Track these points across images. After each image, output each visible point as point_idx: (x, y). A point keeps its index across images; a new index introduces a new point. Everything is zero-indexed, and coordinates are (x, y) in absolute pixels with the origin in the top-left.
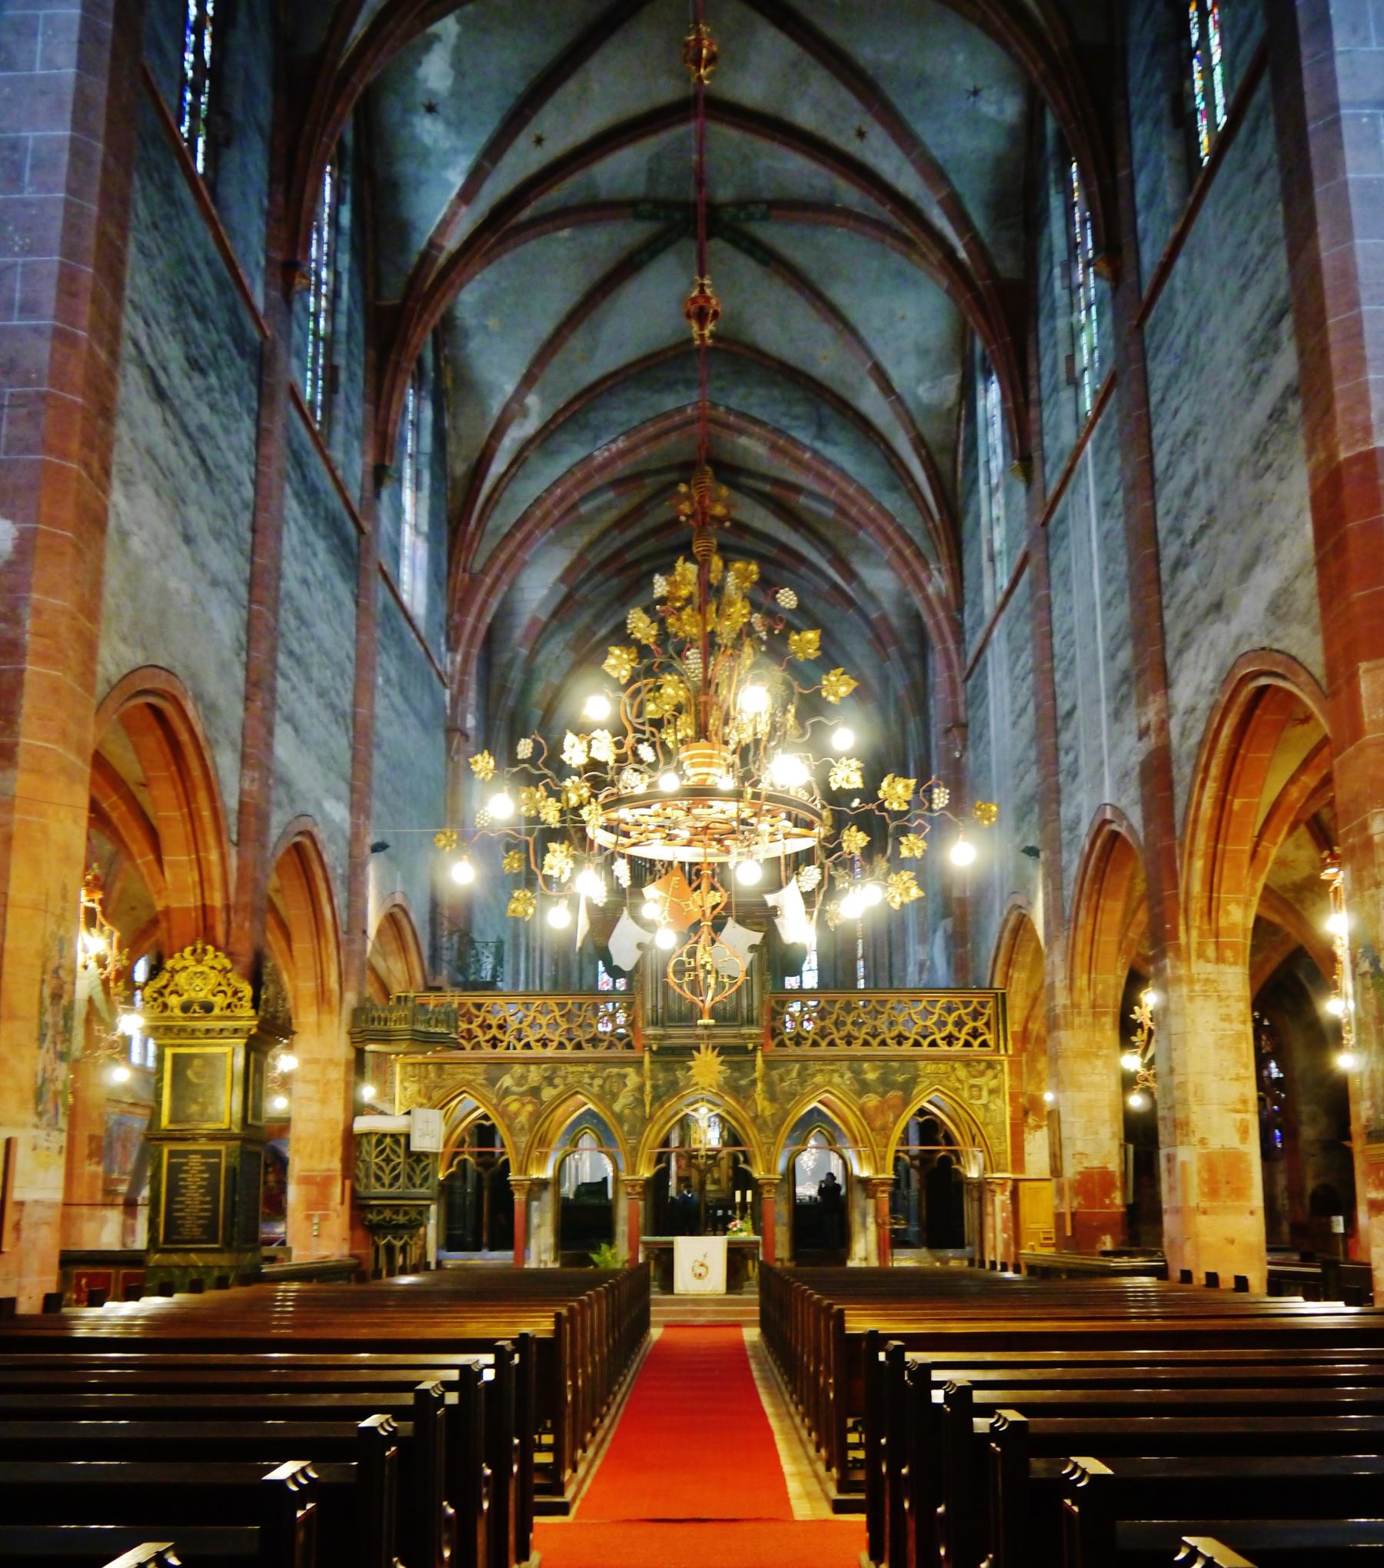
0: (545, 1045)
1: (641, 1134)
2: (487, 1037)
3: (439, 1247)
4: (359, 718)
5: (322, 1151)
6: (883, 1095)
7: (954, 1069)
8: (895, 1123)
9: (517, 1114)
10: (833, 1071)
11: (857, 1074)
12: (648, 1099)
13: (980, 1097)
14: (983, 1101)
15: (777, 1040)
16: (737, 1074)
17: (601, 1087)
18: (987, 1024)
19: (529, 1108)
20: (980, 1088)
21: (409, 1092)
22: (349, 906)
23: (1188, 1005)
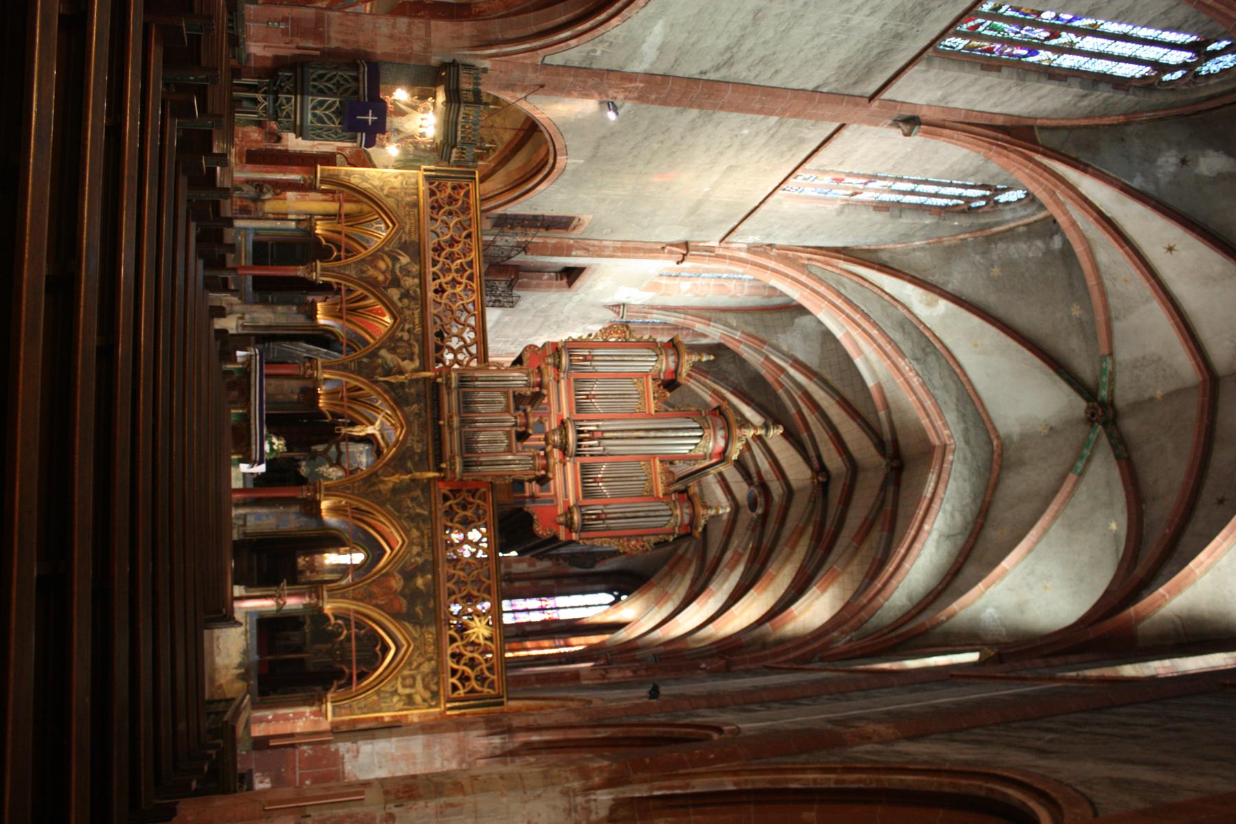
0: (436, 291)
1: (359, 374)
2: (442, 244)
3: (256, 231)
4: (724, 86)
5: (347, 34)
6: (402, 593)
7: (430, 660)
8: (377, 606)
9: (376, 267)
10: (423, 546)
11: (421, 569)
12: (391, 379)
13: (404, 686)
14: (401, 690)
15: (449, 493)
16: (417, 458)
17: (401, 339)
18: (473, 691)
19: (381, 278)
20: (413, 686)
21: (393, 180)
22: (566, 68)
23: (559, 788)
